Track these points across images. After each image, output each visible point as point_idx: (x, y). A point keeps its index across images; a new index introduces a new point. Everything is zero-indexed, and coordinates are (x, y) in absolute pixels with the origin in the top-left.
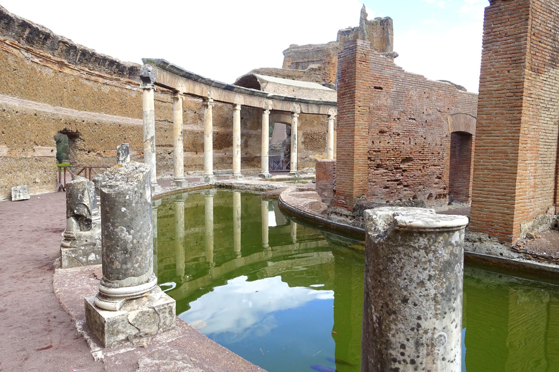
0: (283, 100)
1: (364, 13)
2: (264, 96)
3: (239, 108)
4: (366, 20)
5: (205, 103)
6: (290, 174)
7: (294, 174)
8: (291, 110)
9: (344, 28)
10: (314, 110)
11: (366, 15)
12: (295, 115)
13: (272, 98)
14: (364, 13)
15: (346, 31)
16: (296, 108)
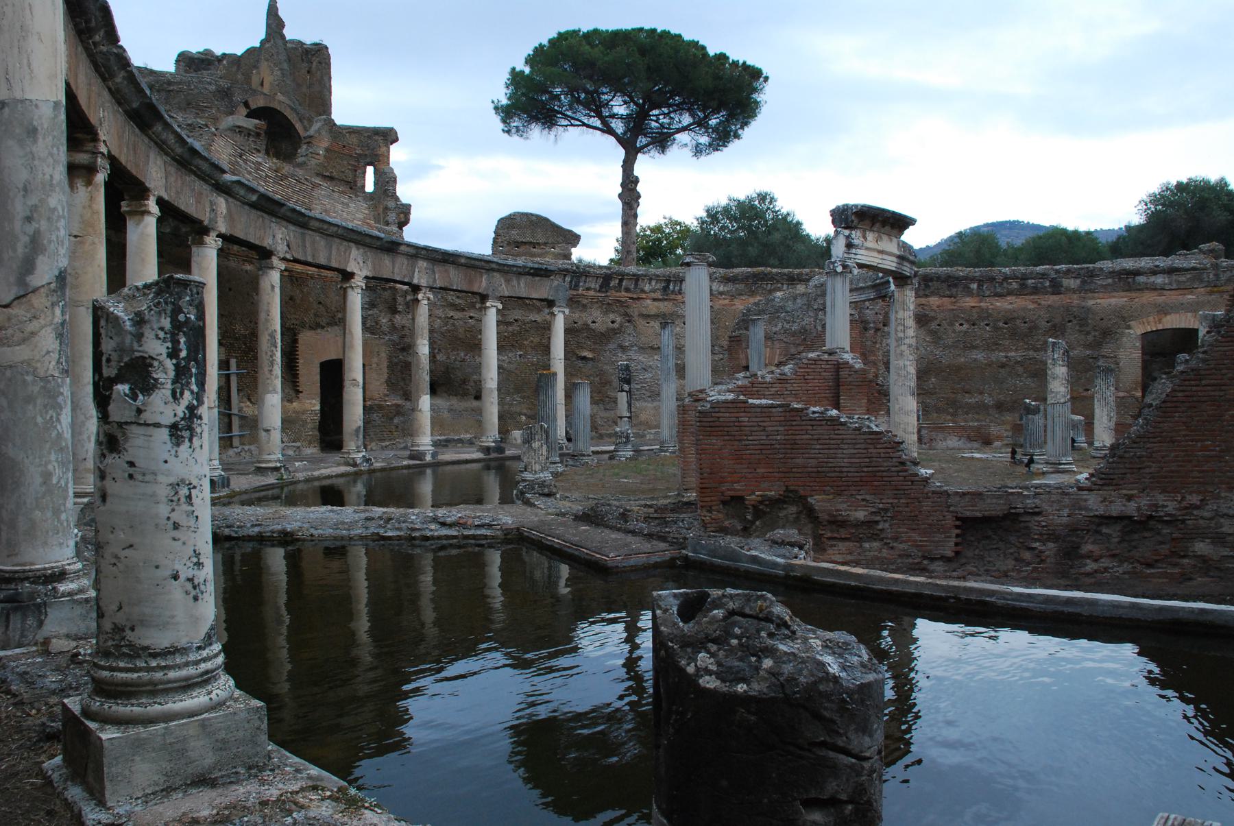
0: (253, 206)
1: (275, 22)
2: (211, 176)
3: (154, 208)
4: (283, 37)
5: (82, 158)
6: (260, 471)
7: (276, 469)
8: (265, 244)
9: (195, 48)
10: (322, 251)
11: (281, 24)
12: (275, 261)
13: (224, 189)
14: (275, 22)
15: (202, 61)
16: (278, 237)
